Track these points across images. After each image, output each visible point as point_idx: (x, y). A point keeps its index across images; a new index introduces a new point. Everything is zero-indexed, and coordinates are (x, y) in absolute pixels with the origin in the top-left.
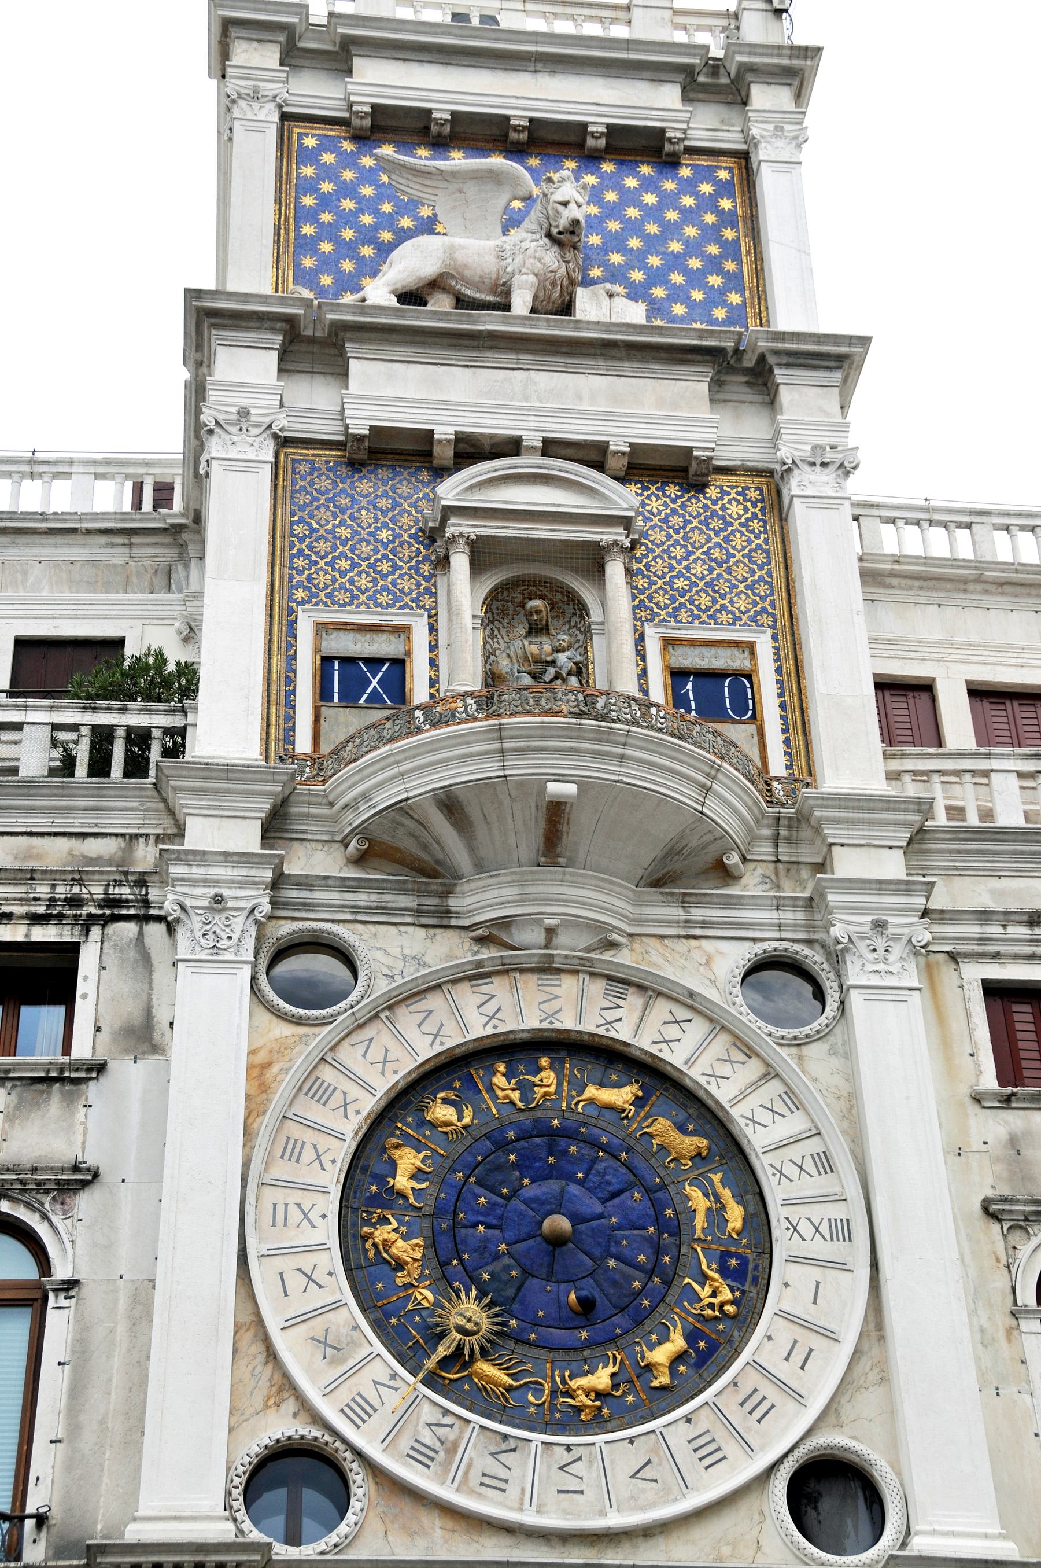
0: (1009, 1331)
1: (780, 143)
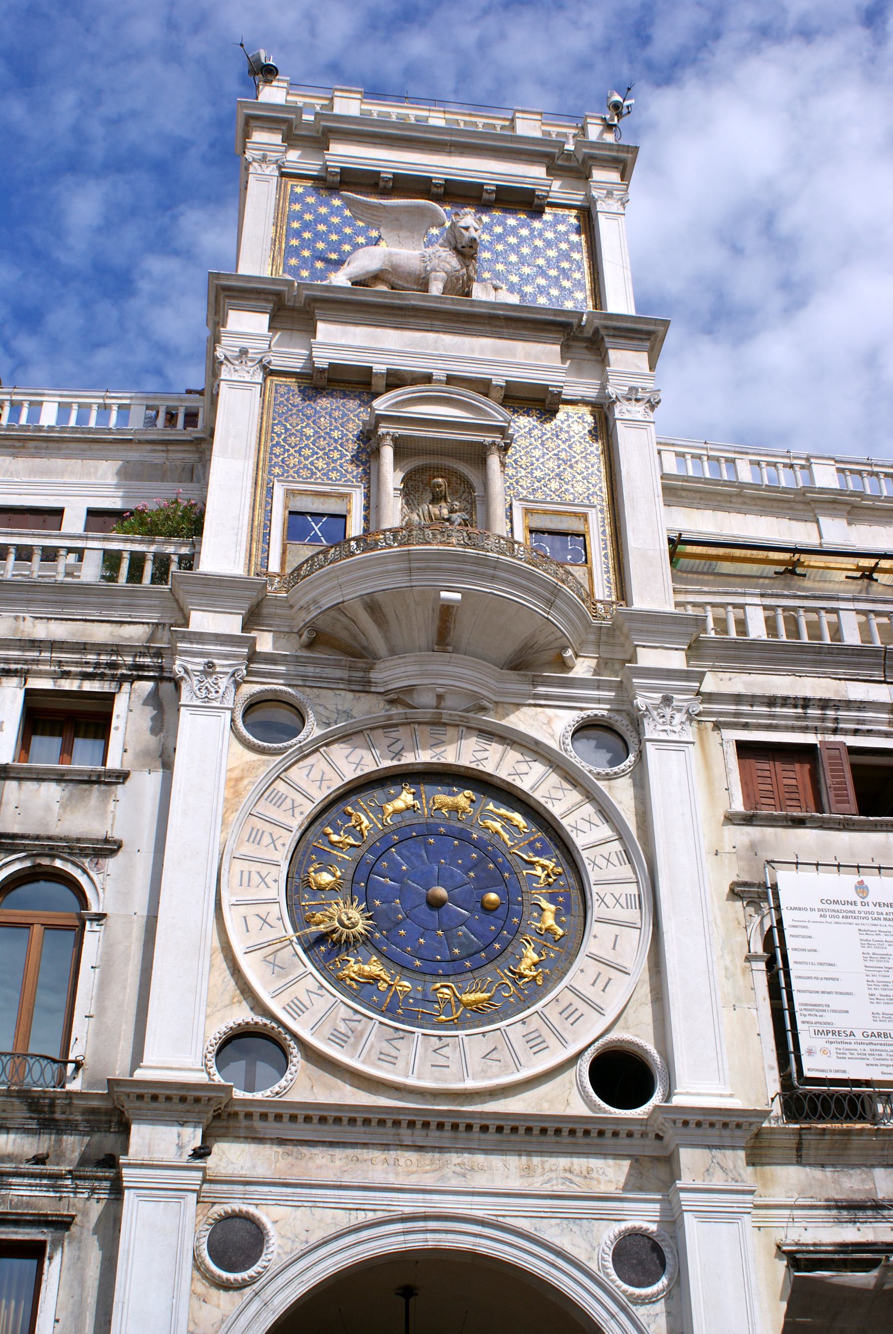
1: (611, 202)
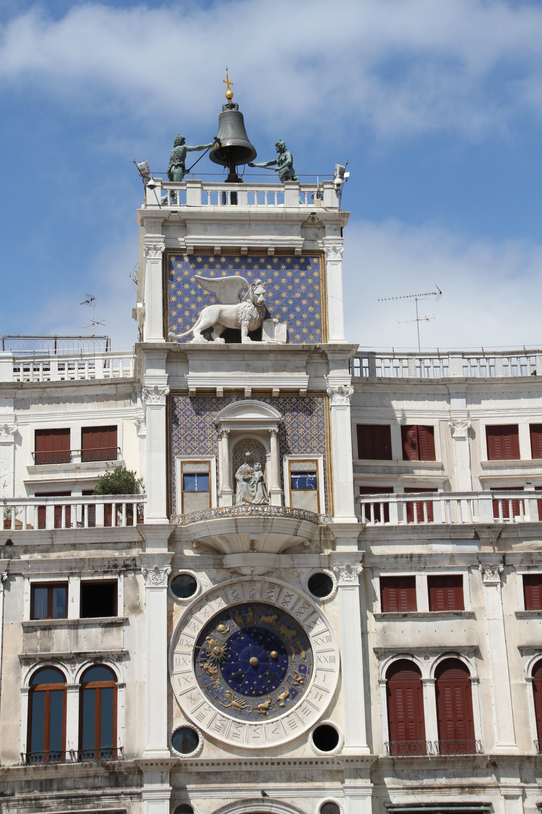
0: (377, 686)
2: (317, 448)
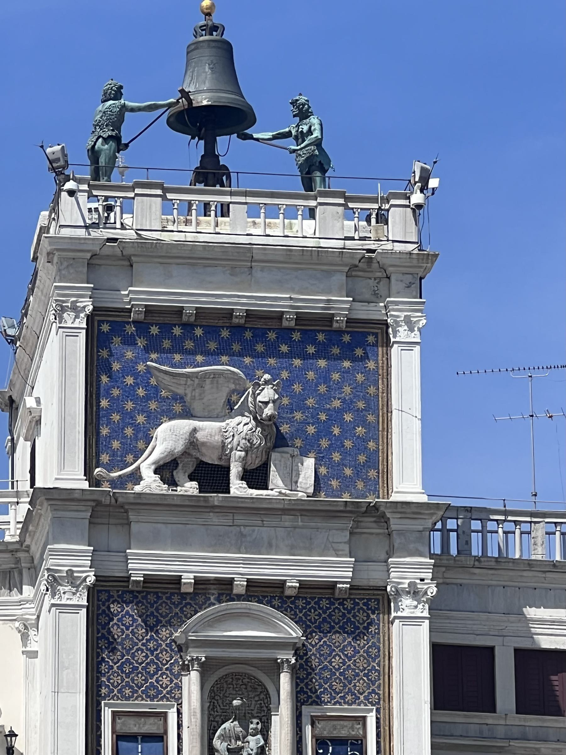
2: (366, 694)
